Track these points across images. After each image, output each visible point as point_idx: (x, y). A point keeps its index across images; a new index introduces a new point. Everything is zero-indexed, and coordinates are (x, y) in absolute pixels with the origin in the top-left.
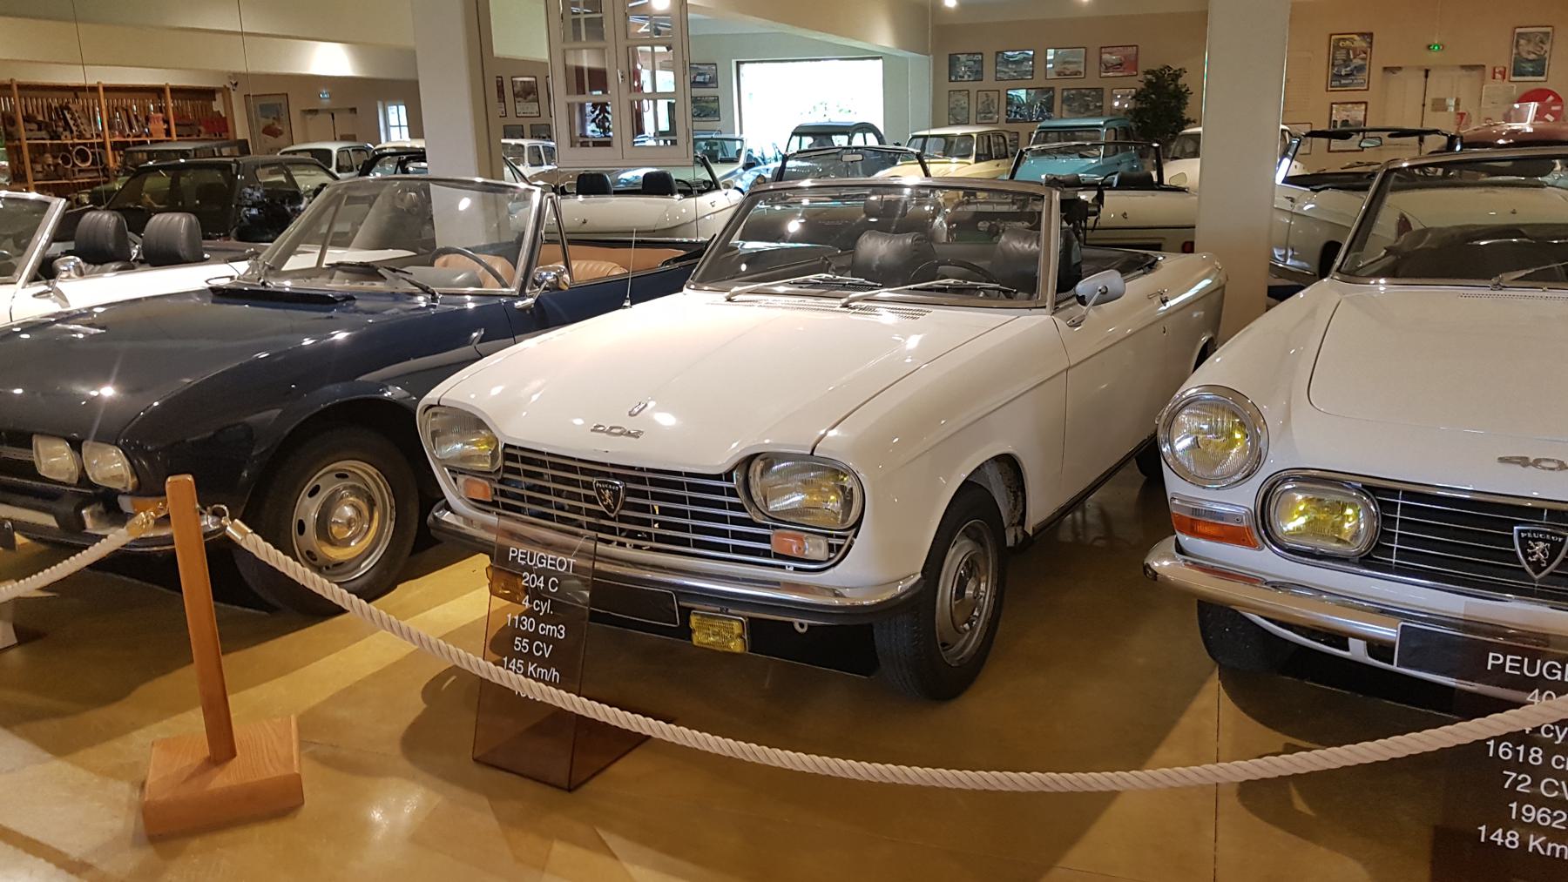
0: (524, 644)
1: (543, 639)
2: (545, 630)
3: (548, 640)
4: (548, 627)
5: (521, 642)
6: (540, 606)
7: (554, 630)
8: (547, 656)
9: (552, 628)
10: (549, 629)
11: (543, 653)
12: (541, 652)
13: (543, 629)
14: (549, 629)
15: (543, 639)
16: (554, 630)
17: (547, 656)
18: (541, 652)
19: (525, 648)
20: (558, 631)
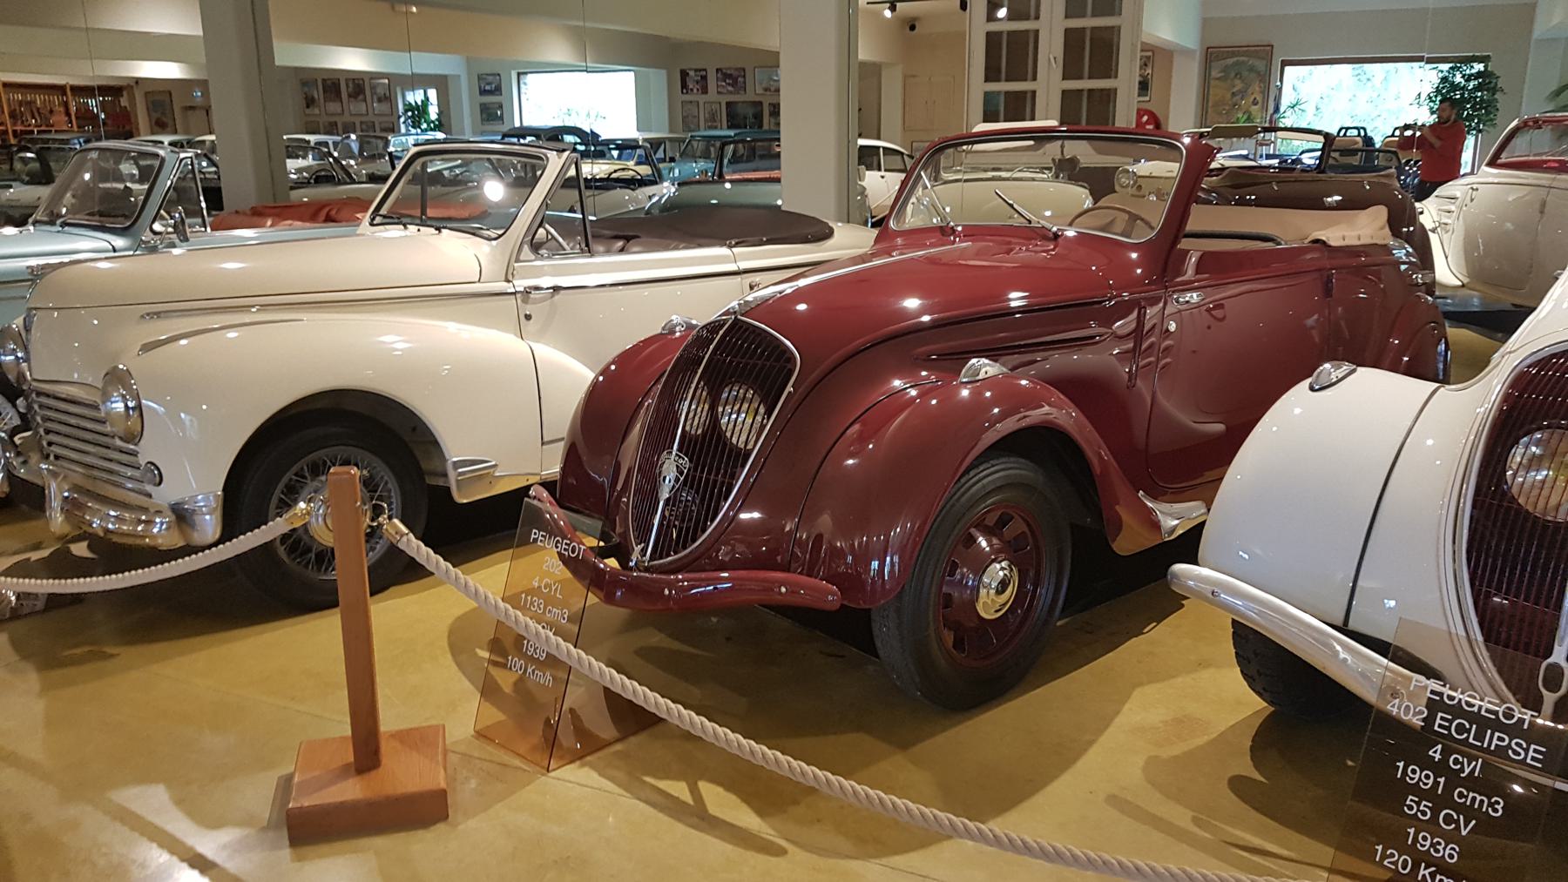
0: (1422, 808)
1: (1459, 808)
2: (1466, 797)
3: (1468, 812)
4: (1471, 795)
5: (1418, 804)
6: (1462, 764)
7: (1482, 802)
8: (1464, 833)
9: (1479, 798)
10: (1474, 799)
11: (1458, 828)
12: (1453, 826)
13: (1461, 795)
14: (1474, 799)
15: (1459, 808)
16: (1482, 802)
17: (1464, 833)
18: (1453, 826)
19: (1424, 813)
20: (1491, 805)
